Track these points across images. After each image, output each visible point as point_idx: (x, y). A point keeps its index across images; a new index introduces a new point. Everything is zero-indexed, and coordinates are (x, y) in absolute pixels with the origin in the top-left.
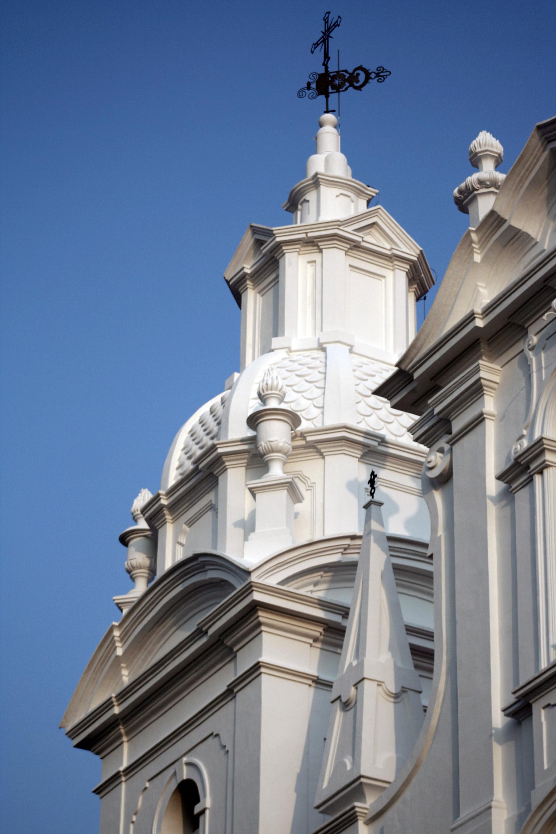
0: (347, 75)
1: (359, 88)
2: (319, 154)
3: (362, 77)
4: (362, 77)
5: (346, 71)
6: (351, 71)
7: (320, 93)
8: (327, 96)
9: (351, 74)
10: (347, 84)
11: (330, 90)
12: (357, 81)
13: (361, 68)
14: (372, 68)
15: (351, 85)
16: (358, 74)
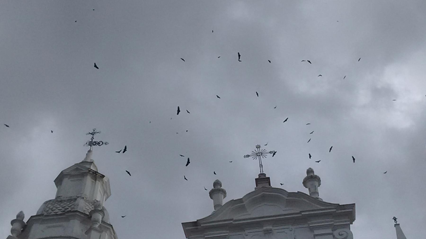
0: (97, 143)
1: (100, 146)
2: (89, 141)
3: (101, 143)
4: (101, 143)
5: (97, 142)
6: (98, 142)
7: (89, 145)
8: (91, 146)
9: (98, 143)
10: (97, 144)
11: (92, 145)
12: (100, 144)
13: (101, 141)
14: (104, 142)
15: (98, 145)
16: (100, 143)
